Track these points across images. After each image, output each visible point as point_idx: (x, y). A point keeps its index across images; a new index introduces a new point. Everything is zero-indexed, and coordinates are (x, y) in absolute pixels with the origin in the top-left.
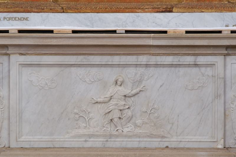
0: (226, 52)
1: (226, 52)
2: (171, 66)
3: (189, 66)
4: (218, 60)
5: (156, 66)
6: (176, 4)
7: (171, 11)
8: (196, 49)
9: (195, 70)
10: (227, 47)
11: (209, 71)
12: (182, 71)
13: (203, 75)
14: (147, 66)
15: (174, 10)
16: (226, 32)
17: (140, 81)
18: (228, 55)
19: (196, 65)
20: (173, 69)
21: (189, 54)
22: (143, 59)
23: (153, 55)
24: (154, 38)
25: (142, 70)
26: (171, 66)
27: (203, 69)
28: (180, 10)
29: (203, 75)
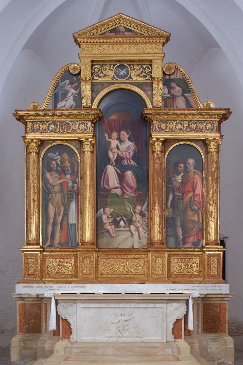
0: (167, 302)
1: (167, 302)
2: (144, 308)
3: (152, 308)
4: (164, 305)
5: (138, 308)
6: (147, 280)
7: (144, 283)
8: (155, 301)
9: (155, 309)
10: (168, 300)
11: (160, 310)
12: (149, 310)
13: (158, 312)
14: (134, 308)
15: (146, 283)
16: (167, 294)
17: (132, 314)
18: (168, 303)
19: (155, 307)
20: (145, 309)
21: (152, 303)
22: (133, 305)
23: (137, 303)
24: (137, 296)
25: (132, 310)
26: (144, 308)
27: (158, 309)
28: (148, 283)
29: (158, 312)
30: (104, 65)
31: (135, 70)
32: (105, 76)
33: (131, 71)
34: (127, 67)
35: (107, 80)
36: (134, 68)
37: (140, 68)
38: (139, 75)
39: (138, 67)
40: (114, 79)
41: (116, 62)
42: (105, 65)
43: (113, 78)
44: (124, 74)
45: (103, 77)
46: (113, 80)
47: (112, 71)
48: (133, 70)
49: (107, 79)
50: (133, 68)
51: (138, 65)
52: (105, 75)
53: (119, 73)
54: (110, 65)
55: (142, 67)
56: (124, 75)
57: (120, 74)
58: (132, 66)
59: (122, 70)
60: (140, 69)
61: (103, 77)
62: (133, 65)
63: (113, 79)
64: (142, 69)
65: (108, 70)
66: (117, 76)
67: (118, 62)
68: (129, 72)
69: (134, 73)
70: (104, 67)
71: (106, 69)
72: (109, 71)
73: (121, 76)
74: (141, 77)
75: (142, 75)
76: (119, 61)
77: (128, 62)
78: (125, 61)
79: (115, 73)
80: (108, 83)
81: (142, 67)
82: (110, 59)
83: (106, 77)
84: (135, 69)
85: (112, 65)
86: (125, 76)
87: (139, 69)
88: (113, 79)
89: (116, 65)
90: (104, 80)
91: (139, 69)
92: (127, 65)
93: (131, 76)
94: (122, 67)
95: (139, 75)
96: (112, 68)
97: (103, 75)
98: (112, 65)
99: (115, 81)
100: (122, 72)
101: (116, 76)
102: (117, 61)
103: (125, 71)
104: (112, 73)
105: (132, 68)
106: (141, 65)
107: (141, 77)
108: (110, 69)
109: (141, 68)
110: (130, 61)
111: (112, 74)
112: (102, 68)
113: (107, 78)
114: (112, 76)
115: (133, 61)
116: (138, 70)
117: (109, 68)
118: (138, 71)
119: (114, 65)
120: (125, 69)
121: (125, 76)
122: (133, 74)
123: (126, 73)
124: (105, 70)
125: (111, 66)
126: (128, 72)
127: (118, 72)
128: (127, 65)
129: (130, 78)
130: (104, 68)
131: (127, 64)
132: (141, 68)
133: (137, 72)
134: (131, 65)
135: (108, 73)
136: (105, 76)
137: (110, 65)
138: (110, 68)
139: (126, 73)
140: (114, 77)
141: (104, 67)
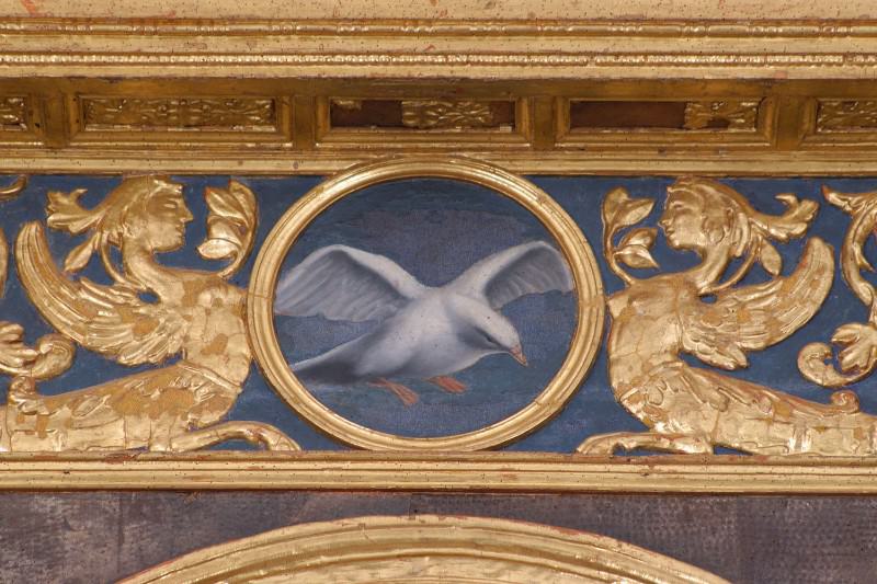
30: (65, 181)
31: (704, 280)
32: (91, 369)
33: (612, 285)
34: (540, 228)
35: (119, 457)
36: (678, 239)
37: (792, 253)
38: (771, 368)
39: (749, 231)
40: (272, 437)
41: (303, 135)
42: (97, 189)
43: (240, 411)
44: (474, 337)
45: (46, 387)
46: (260, 445)
47: (232, 297)
48: (642, 273)
49: (116, 435)
50: (660, 245)
51: (761, 195)
52: (80, 353)
53: (377, 331)
54: (196, 189)
55: (845, 219)
56: (472, 359)
57: (395, 348)
58: (642, 211)
59: (436, 272)
60: (787, 270)
61: (46, 387)
62: (652, 187)
63: (246, 429)
64: (839, 253)
65: (142, 270)
66: (335, 377)
67: (352, 138)
68: (565, 304)
69: (670, 338)
70: (65, 212)
71: (117, 253)
72: (170, 289)
73: (407, 372)
74: (822, 395)
75: (833, 359)
76: (374, 108)
77: (545, 139)
78: (500, 107)
79: (278, 322)
80: (142, 502)
81: (832, 226)
82: (188, 66)
83: (96, 401)
84: (691, 258)
85: (221, 181)
86: (494, 381)
87: (771, 259)
88: (246, 429)
89: (313, 181)
90: (53, 444)
91: (771, 259)
92: (527, 193)
93: (619, 376)
94: (430, 221)
95: (771, 368)
96: (220, 244)
97: (52, 359)
98: (221, 181)
99: (282, 465)
100: (435, 319)
101: (302, 376)
102: (341, 119)
103: (492, 289)
104: (222, 324)
105: (637, 249)
106: (807, 187)
107: (822, 395)
108: (182, 257)
109: (820, 252)
110: (592, 109)
111: (216, 338)
112: (30, 231)
113: (121, 408)
114: (229, 376)
115: (656, 110)
116: (757, 275)
117: (164, 234)
118: (765, 297)
119: (274, 196)
120: (482, 255)
121: (494, 381)
122: (650, 341)
123: (504, 332)
124: (96, 272)
125: (215, 199)
126: (547, 321)
127: (345, 304)
128: (527, 193)
129: (597, 409)
130: (62, 242)
131: (535, 179)
132: (820, 252)
133: (728, 304)
134: (603, 183)
135: (143, 327)
136: (91, 369)
137: (196, 189)
138: (198, 230)
139: (504, 332)
140: (259, 400)
141: (65, 212)
